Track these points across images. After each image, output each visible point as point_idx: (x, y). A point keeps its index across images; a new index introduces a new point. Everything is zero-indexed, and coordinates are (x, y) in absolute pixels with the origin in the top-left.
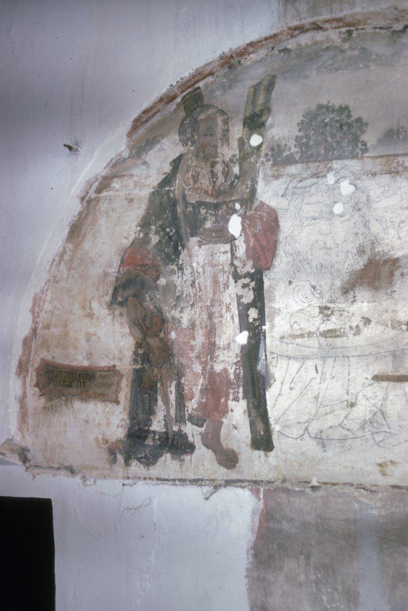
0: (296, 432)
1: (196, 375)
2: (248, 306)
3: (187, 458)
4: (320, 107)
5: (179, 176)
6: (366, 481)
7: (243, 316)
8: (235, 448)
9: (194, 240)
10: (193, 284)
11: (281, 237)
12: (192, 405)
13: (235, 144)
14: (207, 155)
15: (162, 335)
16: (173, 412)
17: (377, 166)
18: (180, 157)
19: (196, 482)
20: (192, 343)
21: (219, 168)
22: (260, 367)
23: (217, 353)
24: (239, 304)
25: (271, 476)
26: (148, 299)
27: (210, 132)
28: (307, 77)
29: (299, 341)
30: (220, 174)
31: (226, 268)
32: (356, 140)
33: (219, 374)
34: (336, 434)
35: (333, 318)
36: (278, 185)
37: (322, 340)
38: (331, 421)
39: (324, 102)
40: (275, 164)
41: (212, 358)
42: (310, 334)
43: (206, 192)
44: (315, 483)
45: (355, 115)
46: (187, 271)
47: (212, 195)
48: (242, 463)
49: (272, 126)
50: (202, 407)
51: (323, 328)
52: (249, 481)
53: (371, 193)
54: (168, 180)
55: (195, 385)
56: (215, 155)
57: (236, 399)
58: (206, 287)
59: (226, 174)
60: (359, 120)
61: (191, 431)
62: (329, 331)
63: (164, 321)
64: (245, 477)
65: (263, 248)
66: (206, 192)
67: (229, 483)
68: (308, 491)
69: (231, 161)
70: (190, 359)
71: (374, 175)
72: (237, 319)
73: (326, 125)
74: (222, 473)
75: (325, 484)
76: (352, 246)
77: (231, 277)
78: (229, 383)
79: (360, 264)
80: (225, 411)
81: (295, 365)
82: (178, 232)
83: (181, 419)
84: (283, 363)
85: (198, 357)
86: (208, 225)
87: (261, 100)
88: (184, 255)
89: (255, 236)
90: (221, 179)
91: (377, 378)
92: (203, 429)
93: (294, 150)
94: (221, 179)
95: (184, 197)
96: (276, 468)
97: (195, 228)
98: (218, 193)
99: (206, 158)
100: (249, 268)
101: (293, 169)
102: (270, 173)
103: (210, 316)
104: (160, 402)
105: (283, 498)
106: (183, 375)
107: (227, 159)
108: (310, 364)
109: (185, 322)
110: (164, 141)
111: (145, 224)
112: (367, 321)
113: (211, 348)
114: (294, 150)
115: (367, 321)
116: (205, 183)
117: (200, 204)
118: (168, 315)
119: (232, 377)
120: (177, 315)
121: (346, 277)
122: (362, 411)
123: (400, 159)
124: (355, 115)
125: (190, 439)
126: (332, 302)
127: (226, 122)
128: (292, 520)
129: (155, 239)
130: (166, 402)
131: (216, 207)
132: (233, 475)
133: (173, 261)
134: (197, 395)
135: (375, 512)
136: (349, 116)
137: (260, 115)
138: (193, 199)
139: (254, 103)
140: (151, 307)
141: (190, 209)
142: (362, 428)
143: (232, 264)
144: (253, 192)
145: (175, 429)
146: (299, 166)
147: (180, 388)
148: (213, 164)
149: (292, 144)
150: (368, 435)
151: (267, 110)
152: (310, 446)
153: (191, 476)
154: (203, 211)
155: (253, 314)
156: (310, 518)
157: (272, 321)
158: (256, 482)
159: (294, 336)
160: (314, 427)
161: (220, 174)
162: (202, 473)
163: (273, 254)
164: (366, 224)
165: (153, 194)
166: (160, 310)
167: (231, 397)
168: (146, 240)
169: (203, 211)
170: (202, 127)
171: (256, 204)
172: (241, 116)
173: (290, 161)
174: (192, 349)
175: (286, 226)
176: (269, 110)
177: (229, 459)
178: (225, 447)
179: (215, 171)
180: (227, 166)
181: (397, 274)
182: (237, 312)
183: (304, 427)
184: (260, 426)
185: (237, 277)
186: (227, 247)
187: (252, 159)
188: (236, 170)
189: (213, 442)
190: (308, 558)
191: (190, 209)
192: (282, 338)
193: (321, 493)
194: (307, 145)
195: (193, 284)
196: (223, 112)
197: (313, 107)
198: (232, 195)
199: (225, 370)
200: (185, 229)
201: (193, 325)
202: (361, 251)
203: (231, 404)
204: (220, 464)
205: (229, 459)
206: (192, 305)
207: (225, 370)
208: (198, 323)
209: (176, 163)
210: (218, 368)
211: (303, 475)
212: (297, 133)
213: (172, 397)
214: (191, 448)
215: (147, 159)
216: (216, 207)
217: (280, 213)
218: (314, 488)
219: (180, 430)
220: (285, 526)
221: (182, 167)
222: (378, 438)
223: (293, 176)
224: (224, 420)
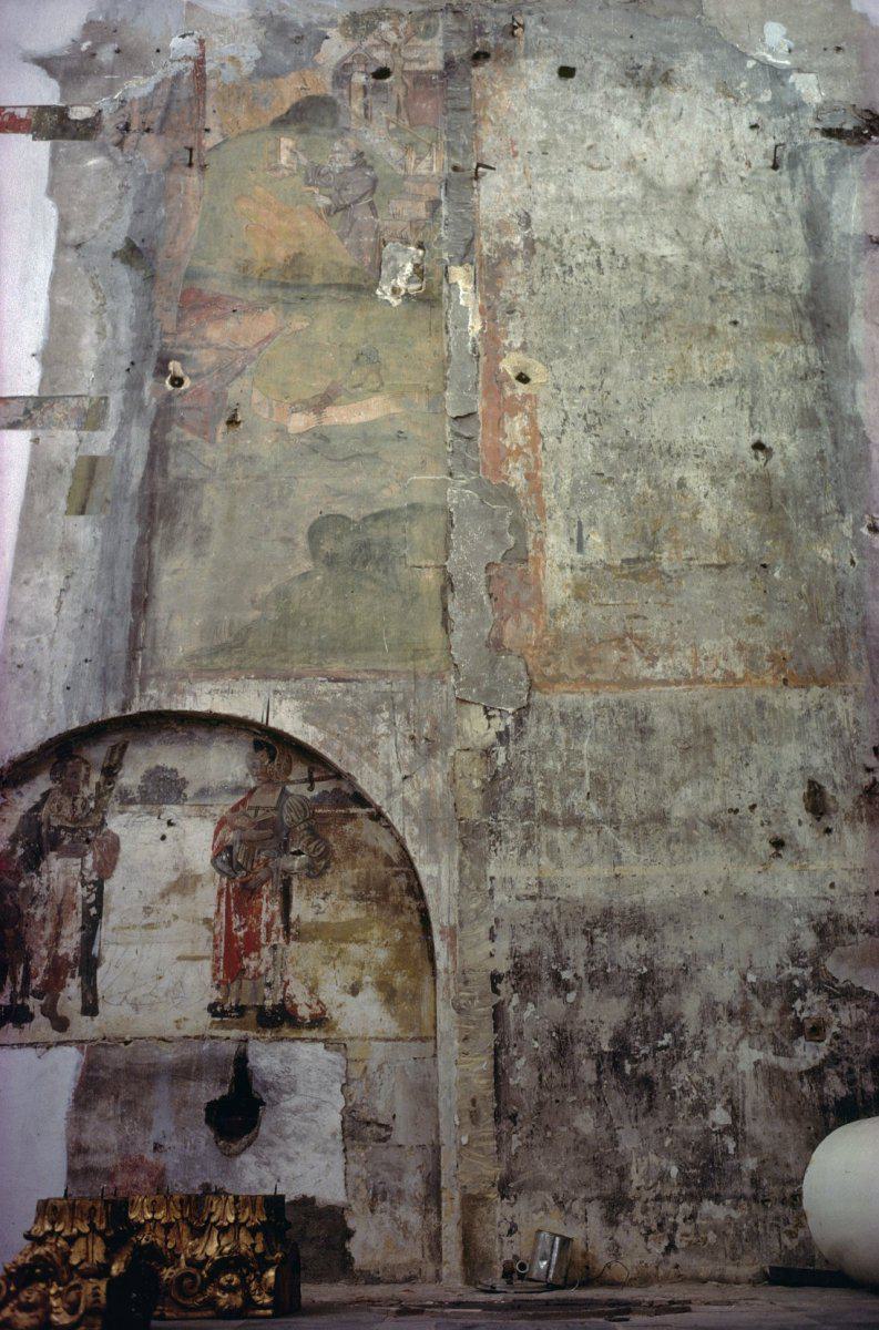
0: (117, 1000)
1: (43, 959)
2: (91, 906)
3: (26, 1025)
4: (158, 767)
5: (46, 806)
6: (165, 1035)
7: (86, 914)
8: (67, 1015)
9: (53, 854)
10: (48, 888)
11: (120, 856)
12: (36, 982)
13: (93, 786)
14: (71, 791)
15: (17, 926)
16: (18, 989)
17: (193, 811)
18: (49, 791)
19: (33, 1045)
20: (42, 933)
21: (79, 802)
22: (95, 951)
23: (62, 940)
24: (83, 904)
25: (95, 1035)
26: (9, 898)
27: (75, 774)
28: (150, 746)
29: (127, 931)
30: (79, 807)
31: (76, 876)
32: (180, 792)
33: (60, 958)
34: (147, 1000)
35: (152, 915)
36: (122, 818)
37: (143, 930)
38: (143, 991)
39: (160, 764)
40: (122, 803)
41: (57, 946)
42: (134, 927)
43: (66, 819)
44: (128, 1038)
45: (181, 776)
46: (45, 878)
47: (70, 822)
48: (71, 1028)
49: (121, 777)
50: (45, 984)
51: (145, 922)
52: (76, 1041)
53: (187, 829)
54: (37, 807)
55: (40, 964)
56: (78, 792)
57: (73, 976)
58: (58, 890)
59: (84, 809)
60: (183, 779)
61: (33, 1004)
62: (149, 925)
63: (20, 915)
64: (73, 1038)
65: (106, 863)
66: (66, 819)
67: (59, 1043)
68: (122, 1045)
69: (89, 798)
70: (39, 946)
71: (190, 817)
72: (80, 915)
73: (160, 780)
74: (55, 1035)
75: (136, 1038)
76: (170, 865)
77: (79, 884)
78: (69, 965)
79: (174, 877)
80: (62, 986)
81: (121, 949)
82: (41, 848)
83: (24, 994)
84: (112, 947)
85: (46, 944)
86: (66, 842)
87: (116, 757)
88: (43, 865)
89: (101, 853)
90: (80, 811)
91: (179, 958)
92: (43, 1001)
93: (136, 795)
94: (80, 811)
95: (49, 821)
96: (99, 1029)
97: (55, 844)
98: (76, 820)
99: (69, 794)
100: (94, 877)
101: (134, 808)
102: (117, 809)
103: (59, 912)
104: (8, 980)
105: (101, 1050)
106: (31, 958)
107: (86, 796)
108: (132, 949)
109: (38, 917)
110: (38, 778)
111: (14, 839)
112: (176, 917)
113: (57, 937)
114: (136, 795)
115: (176, 917)
116: (67, 812)
117: (60, 827)
118: (25, 912)
119: (71, 959)
120: (32, 911)
121: (164, 886)
122: (165, 983)
123: (208, 808)
124: (181, 776)
125: (31, 1010)
126: (152, 903)
127: (88, 769)
128: (108, 1067)
129: (20, 851)
130: (14, 981)
131: (74, 830)
132: (64, 1037)
133: (33, 870)
134: (41, 973)
135: (170, 1056)
136: (177, 775)
137: (114, 768)
138: (56, 823)
139: (111, 759)
140: (11, 904)
141: (52, 831)
142: (166, 995)
143: (81, 874)
144: (103, 823)
145: (19, 1002)
146: (139, 806)
147: (27, 970)
148: (75, 799)
149: (135, 790)
150: (170, 1000)
151: (119, 765)
152: (126, 1010)
153: (29, 1041)
154: (63, 833)
155: (93, 911)
156: (121, 1065)
157: (107, 916)
158: (82, 1042)
159: (122, 928)
160: (131, 996)
161: (79, 807)
162: (39, 1037)
163: (113, 868)
164: (181, 851)
165: (23, 817)
166: (17, 907)
167: (69, 974)
168: (13, 851)
169: (63, 833)
170: (69, 771)
171: (104, 830)
172: (100, 766)
173: (132, 802)
174: (41, 937)
175: (125, 847)
176: (121, 765)
177: (61, 1024)
178: (59, 1014)
179: (75, 803)
180: (85, 801)
181: (199, 886)
182: (80, 909)
183: (123, 996)
184: (90, 997)
185: (84, 884)
186: (79, 860)
187: (105, 798)
188: (92, 805)
189: (50, 1012)
190: (117, 1097)
191: (52, 831)
192: (114, 929)
193: (131, 1045)
194: (145, 792)
195: (48, 888)
196: (86, 762)
197: (153, 766)
198: (86, 823)
199: (67, 955)
200: (46, 845)
201: (44, 919)
202: (176, 869)
203: (69, 980)
204: (54, 1028)
205: (61, 1024)
206: (46, 904)
207: (67, 955)
208: (48, 917)
209: (45, 796)
210: (61, 952)
211: (119, 1033)
212: (139, 783)
213: (20, 977)
214: (30, 1017)
215: (22, 790)
216: (74, 830)
217: (122, 839)
218: (126, 1043)
219: (23, 1004)
220: (102, 1073)
221: (50, 799)
222: (177, 1001)
223: (134, 813)
224: (61, 993)
